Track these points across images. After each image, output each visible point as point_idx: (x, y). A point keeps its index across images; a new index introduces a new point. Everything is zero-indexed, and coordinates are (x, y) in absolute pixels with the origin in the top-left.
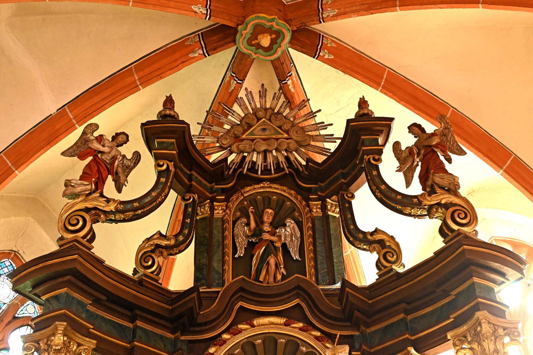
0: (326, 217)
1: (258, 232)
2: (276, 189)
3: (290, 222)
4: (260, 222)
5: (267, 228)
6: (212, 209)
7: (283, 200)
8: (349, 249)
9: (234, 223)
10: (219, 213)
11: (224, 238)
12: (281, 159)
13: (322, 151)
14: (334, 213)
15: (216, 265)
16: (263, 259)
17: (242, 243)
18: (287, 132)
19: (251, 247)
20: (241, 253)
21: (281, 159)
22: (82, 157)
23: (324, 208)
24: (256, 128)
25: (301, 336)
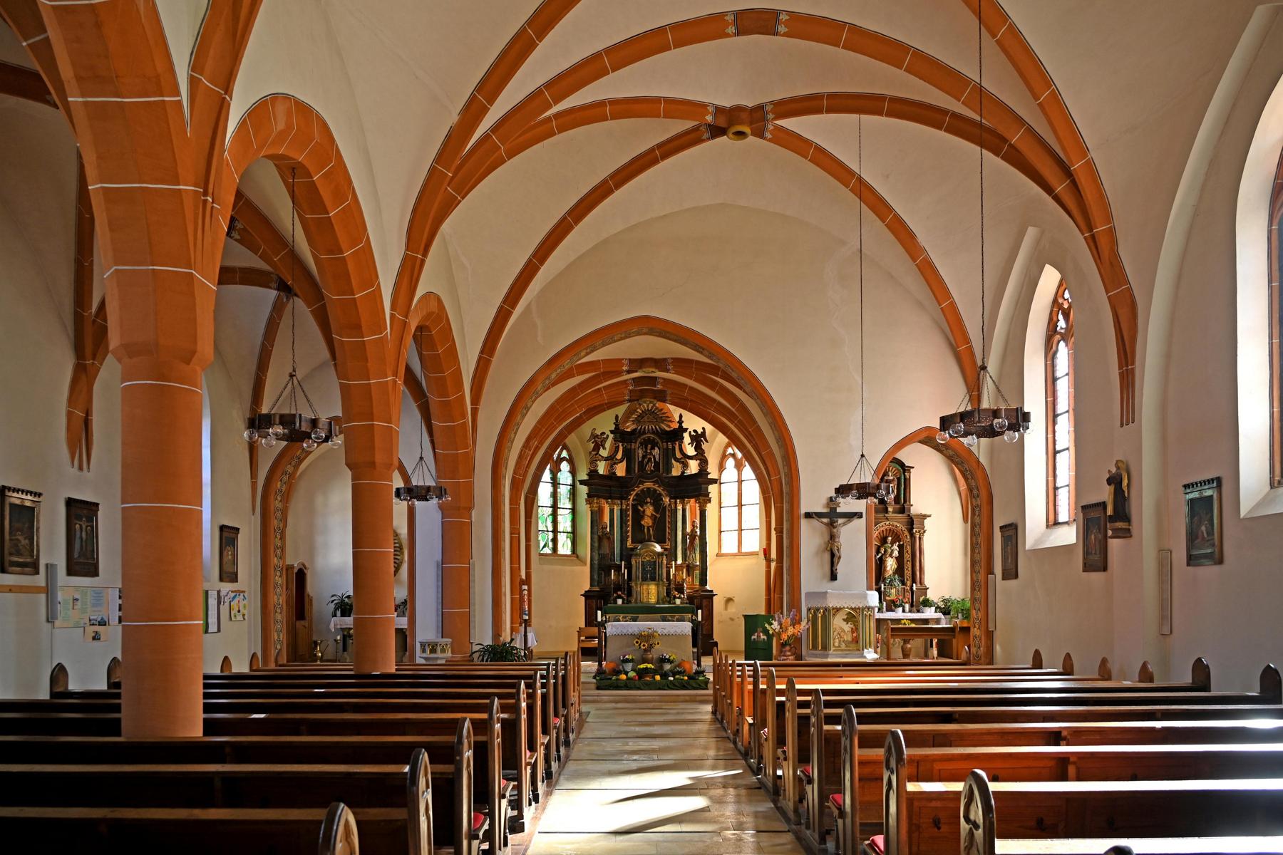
0: (667, 448)
1: (646, 452)
2: (652, 436)
3: (656, 448)
4: (646, 448)
5: (649, 451)
6: (631, 445)
7: (654, 439)
8: (673, 461)
9: (639, 447)
10: (633, 447)
11: (635, 455)
12: (654, 427)
13: (669, 427)
14: (670, 447)
15: (633, 466)
16: (647, 463)
17: (641, 455)
18: (656, 419)
19: (644, 457)
20: (640, 459)
21: (654, 427)
22: (593, 443)
23: (667, 445)
24: (646, 418)
25: (657, 488)
